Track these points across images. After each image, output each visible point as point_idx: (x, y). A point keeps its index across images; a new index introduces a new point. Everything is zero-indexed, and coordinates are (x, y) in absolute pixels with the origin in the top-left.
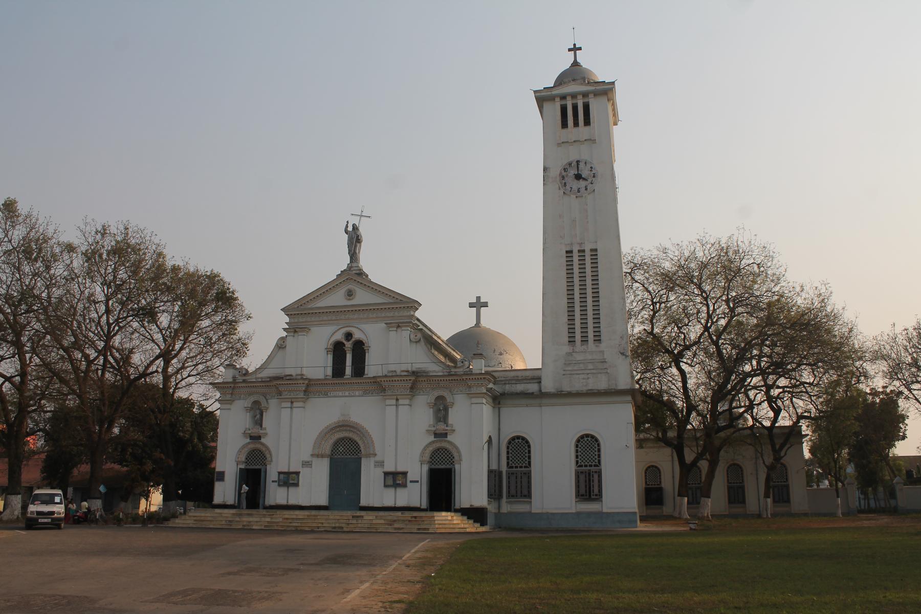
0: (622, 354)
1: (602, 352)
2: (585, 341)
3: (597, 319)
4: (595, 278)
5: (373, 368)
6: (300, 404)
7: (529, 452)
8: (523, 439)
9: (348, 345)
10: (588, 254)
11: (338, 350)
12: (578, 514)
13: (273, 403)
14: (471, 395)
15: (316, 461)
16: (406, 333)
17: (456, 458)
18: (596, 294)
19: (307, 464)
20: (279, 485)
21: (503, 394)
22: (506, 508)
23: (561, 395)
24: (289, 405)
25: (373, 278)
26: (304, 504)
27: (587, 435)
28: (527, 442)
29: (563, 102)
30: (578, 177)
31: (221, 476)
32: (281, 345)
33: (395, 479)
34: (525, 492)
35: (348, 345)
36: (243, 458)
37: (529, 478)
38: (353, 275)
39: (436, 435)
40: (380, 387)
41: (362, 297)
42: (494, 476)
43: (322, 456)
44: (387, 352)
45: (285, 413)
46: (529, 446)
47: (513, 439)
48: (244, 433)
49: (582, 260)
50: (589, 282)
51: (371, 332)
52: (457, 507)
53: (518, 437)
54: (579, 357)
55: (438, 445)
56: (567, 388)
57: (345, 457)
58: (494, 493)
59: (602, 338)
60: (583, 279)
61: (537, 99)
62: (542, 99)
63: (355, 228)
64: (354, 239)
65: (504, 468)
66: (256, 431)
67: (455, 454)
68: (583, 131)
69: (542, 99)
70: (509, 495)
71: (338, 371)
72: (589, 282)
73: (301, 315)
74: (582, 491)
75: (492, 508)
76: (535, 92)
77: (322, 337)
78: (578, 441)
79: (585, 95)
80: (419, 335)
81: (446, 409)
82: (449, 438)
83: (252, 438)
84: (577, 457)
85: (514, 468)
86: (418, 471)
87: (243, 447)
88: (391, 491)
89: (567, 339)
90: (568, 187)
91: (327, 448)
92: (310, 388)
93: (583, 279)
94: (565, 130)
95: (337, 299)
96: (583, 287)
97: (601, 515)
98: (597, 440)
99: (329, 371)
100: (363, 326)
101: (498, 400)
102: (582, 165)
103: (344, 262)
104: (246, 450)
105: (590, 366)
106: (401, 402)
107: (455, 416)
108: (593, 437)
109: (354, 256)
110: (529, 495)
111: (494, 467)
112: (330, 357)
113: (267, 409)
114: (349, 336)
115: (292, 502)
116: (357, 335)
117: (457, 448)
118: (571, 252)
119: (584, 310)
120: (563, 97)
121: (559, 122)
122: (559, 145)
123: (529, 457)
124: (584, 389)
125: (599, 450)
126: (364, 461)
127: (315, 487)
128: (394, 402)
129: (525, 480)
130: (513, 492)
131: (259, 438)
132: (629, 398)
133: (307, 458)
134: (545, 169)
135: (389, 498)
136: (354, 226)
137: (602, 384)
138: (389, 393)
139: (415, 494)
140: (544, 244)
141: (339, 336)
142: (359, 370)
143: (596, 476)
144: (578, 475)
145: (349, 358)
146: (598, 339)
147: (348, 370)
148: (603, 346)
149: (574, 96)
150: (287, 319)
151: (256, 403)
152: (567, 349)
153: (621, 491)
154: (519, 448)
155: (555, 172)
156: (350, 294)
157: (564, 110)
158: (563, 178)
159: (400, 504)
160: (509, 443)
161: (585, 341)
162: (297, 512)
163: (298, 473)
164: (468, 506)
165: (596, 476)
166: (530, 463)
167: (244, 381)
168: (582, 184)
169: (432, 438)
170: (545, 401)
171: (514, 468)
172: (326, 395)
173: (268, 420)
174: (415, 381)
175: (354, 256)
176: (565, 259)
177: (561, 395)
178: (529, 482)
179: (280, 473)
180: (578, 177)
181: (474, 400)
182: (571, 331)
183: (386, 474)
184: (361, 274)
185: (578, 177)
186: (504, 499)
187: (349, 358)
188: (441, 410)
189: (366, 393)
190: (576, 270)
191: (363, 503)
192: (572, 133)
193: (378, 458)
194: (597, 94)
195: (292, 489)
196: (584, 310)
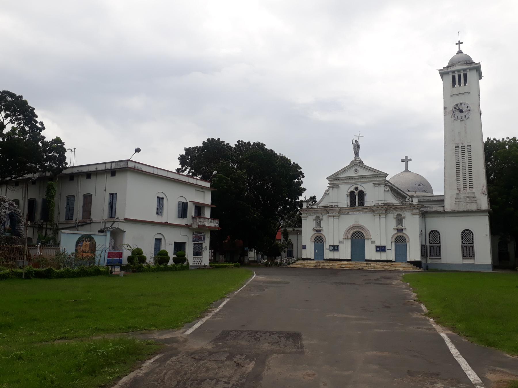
0: (483, 194)
1: (474, 193)
2: (465, 187)
3: (471, 178)
4: (470, 159)
5: (369, 201)
6: (337, 218)
7: (440, 237)
8: (437, 231)
9: (356, 192)
10: (466, 147)
11: (352, 195)
12: (463, 264)
13: (325, 217)
14: (413, 214)
15: (344, 240)
16: (382, 188)
17: (407, 240)
18: (470, 166)
19: (341, 242)
20: (330, 250)
21: (427, 212)
22: (429, 261)
23: (454, 213)
24: (332, 218)
25: (366, 163)
26: (341, 258)
27: (467, 230)
28: (438, 233)
29: (453, 74)
30: (461, 111)
31: (304, 247)
32: (326, 194)
33: (381, 249)
34: (438, 254)
35: (356, 192)
36: (313, 239)
37: (440, 248)
38: (357, 163)
39: (398, 230)
40: (372, 210)
41: (362, 172)
42: (423, 248)
43: (348, 239)
44: (374, 195)
45: (331, 221)
46: (439, 235)
47: (432, 231)
48: (314, 230)
49: (463, 150)
50: (467, 161)
51: (367, 188)
52: (408, 260)
53: (434, 231)
54: (462, 195)
55: (399, 234)
56: (457, 209)
57: (358, 238)
58: (424, 254)
59: (473, 186)
60: (463, 159)
61: (440, 73)
62: (443, 73)
63: (356, 141)
64: (357, 147)
65: (428, 244)
66: (318, 228)
67: (407, 238)
68: (462, 88)
69: (443, 73)
70: (431, 256)
71: (352, 204)
72: (467, 161)
73: (335, 180)
74: (465, 254)
75: (424, 262)
76: (439, 70)
77: (345, 189)
78: (463, 232)
79: (465, 70)
80: (388, 188)
81: (401, 220)
82: (404, 231)
83: (316, 231)
84: (462, 239)
85: (432, 245)
86: (391, 246)
87: (313, 235)
88: (379, 253)
89: (456, 187)
90: (456, 116)
91: (349, 237)
92: (341, 211)
93: (463, 159)
94: (454, 88)
95: (351, 173)
96: (464, 163)
97: (474, 265)
98: (471, 232)
99: (349, 204)
100: (363, 185)
101: (424, 215)
102: (463, 105)
103: (352, 157)
104: (314, 236)
105: (468, 199)
106: (381, 216)
107: (405, 223)
108: (469, 231)
109: (357, 154)
110: (440, 255)
111: (424, 243)
112: (349, 198)
113: (322, 219)
114: (356, 189)
115: (335, 258)
116: (360, 188)
117: (407, 236)
118: (458, 147)
119: (464, 174)
120: (453, 72)
121: (452, 85)
122: (451, 96)
123: (440, 239)
124: (465, 210)
125: (473, 237)
126: (366, 241)
127: (345, 252)
128: (378, 216)
129: (438, 249)
130: (432, 254)
131: (320, 231)
132: (487, 214)
133: (342, 240)
134: (445, 108)
135: (378, 256)
136: (356, 141)
137: (474, 207)
138: (376, 213)
139: (390, 255)
140: (445, 144)
141: (352, 189)
142: (362, 202)
143: (471, 248)
144: (463, 248)
145: (357, 199)
146: (471, 187)
147: (357, 204)
148: (474, 190)
149: (459, 71)
150: (329, 182)
151: (318, 217)
152: (457, 192)
153: (484, 253)
154: (435, 236)
155: (450, 109)
156: (356, 171)
157: (454, 78)
158: (454, 112)
159: (383, 259)
160: (430, 233)
161: (465, 187)
162: (342, 262)
163: (338, 246)
164: (413, 260)
165: (471, 248)
166: (440, 242)
167: (312, 208)
168: (463, 115)
169: (396, 232)
170: (446, 215)
171: (432, 245)
172: (348, 213)
173: (323, 224)
174: (387, 207)
175: (357, 154)
176: (455, 150)
177: (454, 213)
178: (440, 250)
179: (330, 246)
180: (461, 111)
181: (414, 216)
182: (458, 183)
183: (377, 247)
184: (361, 162)
185: (461, 111)
186: (429, 257)
187: (357, 199)
188: (400, 220)
189: (365, 213)
190: (460, 156)
191: (367, 258)
192: (458, 89)
193: (372, 240)
194: (470, 69)
195: (336, 253)
196: (464, 174)
